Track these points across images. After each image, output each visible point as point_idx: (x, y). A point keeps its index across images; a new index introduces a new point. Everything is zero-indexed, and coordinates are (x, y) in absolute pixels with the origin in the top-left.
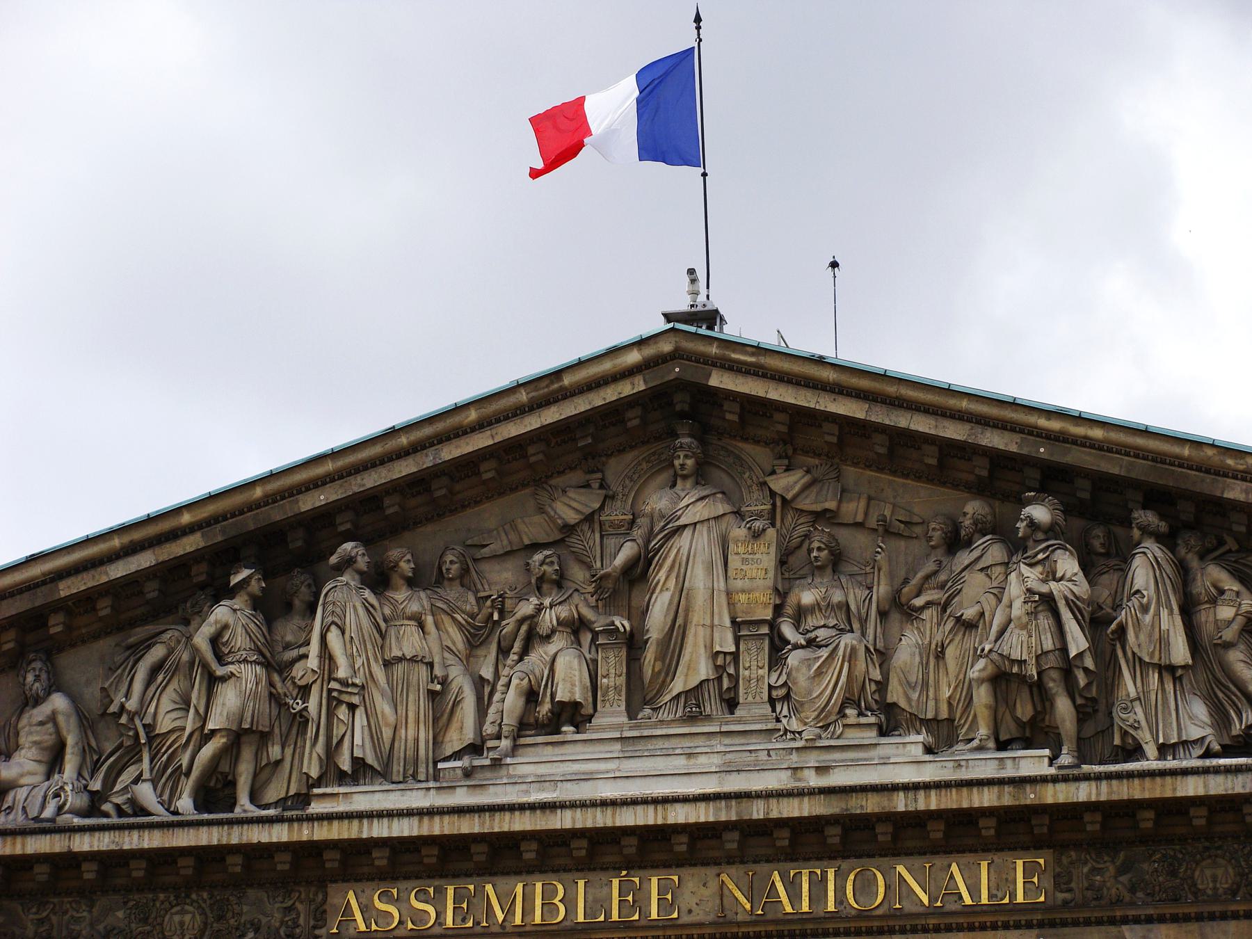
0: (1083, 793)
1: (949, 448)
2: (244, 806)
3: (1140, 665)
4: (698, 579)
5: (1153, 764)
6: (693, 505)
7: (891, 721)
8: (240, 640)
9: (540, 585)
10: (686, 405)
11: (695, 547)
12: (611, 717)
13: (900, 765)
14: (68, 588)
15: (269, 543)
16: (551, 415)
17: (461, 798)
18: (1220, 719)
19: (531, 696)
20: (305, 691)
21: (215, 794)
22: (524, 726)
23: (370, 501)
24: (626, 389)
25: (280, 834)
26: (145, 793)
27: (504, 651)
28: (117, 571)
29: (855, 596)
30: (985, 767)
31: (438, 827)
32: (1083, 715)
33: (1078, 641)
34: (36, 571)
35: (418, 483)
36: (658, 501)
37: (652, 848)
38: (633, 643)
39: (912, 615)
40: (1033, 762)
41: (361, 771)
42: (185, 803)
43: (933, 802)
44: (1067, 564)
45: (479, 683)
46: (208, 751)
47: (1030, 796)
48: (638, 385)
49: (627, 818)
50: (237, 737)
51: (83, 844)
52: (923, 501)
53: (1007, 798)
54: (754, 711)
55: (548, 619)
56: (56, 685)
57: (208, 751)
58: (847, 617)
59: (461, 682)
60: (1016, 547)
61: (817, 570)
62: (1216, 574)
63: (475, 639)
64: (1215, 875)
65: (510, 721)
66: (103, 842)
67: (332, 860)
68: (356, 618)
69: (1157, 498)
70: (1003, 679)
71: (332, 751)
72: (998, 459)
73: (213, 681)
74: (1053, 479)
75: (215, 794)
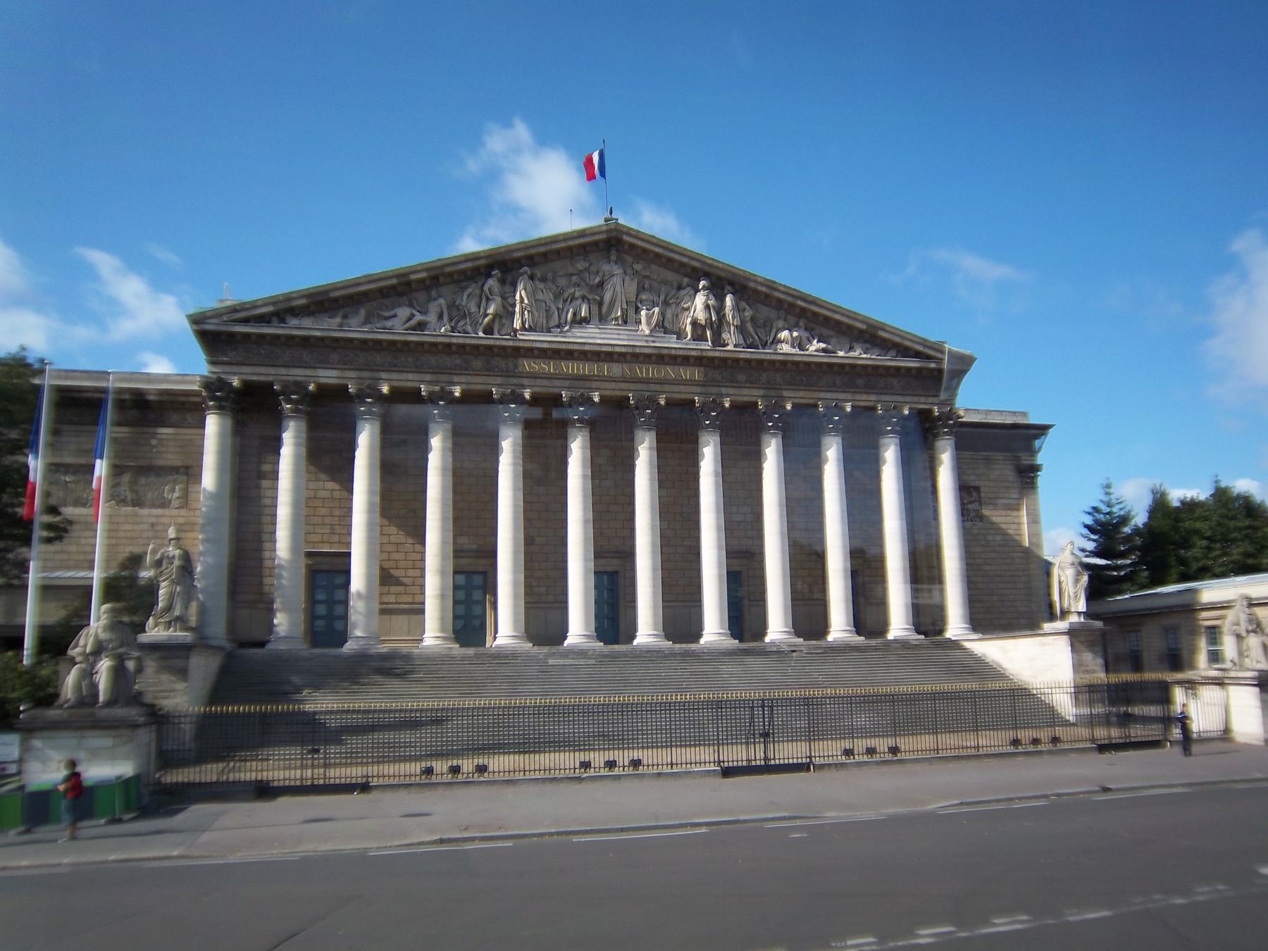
0: (717, 354)
1: (682, 264)
4: (618, 288)
5: (730, 348)
6: (618, 270)
10: (612, 244)
11: (617, 280)
13: (671, 342)
14: (448, 270)
16: (582, 241)
19: (575, 314)
25: (511, 343)
26: (469, 328)
27: (565, 301)
28: (462, 267)
31: (554, 346)
32: (713, 335)
34: (439, 264)
35: (544, 255)
36: (606, 267)
38: (600, 304)
41: (531, 329)
42: (481, 334)
43: (681, 353)
46: (487, 319)
47: (704, 354)
48: (604, 236)
52: (670, 276)
56: (440, 296)
57: (487, 319)
59: (553, 308)
62: (743, 304)
63: (557, 296)
64: (741, 377)
66: (461, 341)
67: (522, 352)
69: (731, 283)
72: (694, 269)
73: (488, 299)
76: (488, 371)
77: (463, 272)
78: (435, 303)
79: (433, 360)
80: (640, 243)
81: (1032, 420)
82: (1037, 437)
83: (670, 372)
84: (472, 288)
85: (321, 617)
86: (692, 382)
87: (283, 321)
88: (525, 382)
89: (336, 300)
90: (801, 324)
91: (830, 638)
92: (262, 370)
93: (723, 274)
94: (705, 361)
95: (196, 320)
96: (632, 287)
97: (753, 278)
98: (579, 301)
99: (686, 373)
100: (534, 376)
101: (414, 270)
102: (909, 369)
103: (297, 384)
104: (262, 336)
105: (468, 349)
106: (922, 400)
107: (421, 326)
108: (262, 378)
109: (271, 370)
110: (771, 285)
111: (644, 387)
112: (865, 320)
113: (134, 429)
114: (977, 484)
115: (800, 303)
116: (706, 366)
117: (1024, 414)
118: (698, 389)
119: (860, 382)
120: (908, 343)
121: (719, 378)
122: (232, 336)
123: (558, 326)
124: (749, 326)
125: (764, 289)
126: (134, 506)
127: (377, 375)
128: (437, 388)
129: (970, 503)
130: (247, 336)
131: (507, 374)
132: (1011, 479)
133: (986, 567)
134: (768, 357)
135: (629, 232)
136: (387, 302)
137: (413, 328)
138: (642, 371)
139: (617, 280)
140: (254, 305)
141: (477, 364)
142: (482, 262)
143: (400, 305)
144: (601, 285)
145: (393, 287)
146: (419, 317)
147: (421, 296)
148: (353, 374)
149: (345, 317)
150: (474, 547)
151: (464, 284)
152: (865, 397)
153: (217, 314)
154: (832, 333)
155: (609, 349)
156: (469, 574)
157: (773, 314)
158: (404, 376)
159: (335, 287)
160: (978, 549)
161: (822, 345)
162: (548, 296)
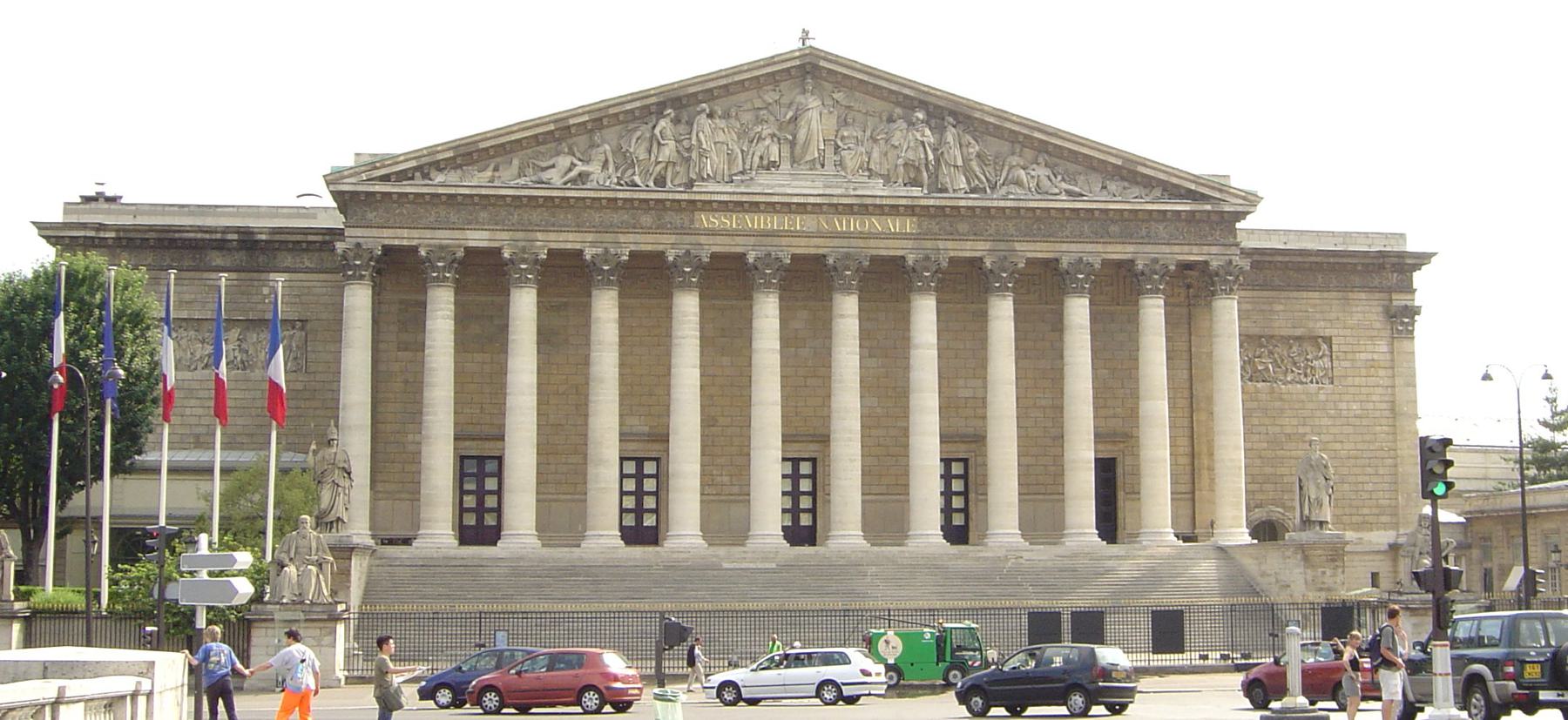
0: (931, 202)
3: (947, 163)
4: (814, 124)
6: (814, 102)
7: (872, 174)
8: (669, 133)
9: (761, 121)
10: (809, 70)
11: (814, 115)
12: (785, 166)
14: (611, 111)
15: (679, 103)
16: (769, 70)
18: (968, 182)
20: (689, 150)
21: (660, 181)
22: (760, 167)
23: (710, 90)
25: (685, 197)
26: (637, 179)
28: (628, 107)
29: (860, 134)
33: (931, 157)
36: (800, 99)
37: (802, 208)
38: (793, 144)
39: (876, 141)
40: (916, 192)
43: (888, 202)
44: (928, 132)
46: (659, 168)
47: (916, 202)
49: (795, 200)
52: (878, 105)
53: (910, 202)
54: (830, 169)
56: (604, 141)
57: (659, 168)
58: (858, 142)
60: (911, 124)
61: (846, 123)
63: (742, 134)
64: (963, 227)
66: (627, 195)
68: (707, 129)
69: (953, 113)
70: (905, 165)
72: (906, 96)
74: (923, 105)
75: (660, 181)
76: (660, 228)
77: (632, 111)
78: (601, 149)
79: (597, 217)
80: (839, 69)
81: (1412, 246)
82: (1417, 267)
83: (876, 223)
84: (644, 130)
85: (469, 510)
86: (903, 236)
87: (426, 176)
88: (703, 240)
89: (486, 149)
90: (1040, 160)
91: (1070, 544)
92: (405, 233)
93: (940, 103)
94: (917, 210)
95: (332, 179)
96: (832, 122)
97: (980, 107)
98: (768, 142)
99: (894, 224)
100: (713, 233)
101: (573, 113)
102: (1179, 212)
103: (442, 247)
104: (400, 195)
105: (636, 204)
106: (1195, 249)
107: (583, 177)
108: (405, 243)
109: (415, 234)
110: (1001, 115)
111: (845, 242)
112: (1118, 154)
113: (243, 275)
114: (1327, 333)
115: (1037, 135)
116: (919, 216)
117: (1402, 236)
118: (910, 244)
119: (1114, 229)
120: (1175, 181)
121: (936, 229)
122: (373, 194)
123: (742, 173)
124: (974, 164)
125: (992, 120)
126: (244, 369)
127: (531, 235)
128: (600, 251)
129: (1317, 358)
130: (390, 194)
131: (682, 231)
132: (1378, 325)
133: (1338, 446)
134: (995, 204)
135: (827, 57)
136: (542, 148)
137: (573, 181)
138: (842, 224)
139: (814, 115)
140: (394, 159)
141: (646, 219)
142: (653, 100)
143: (558, 154)
144: (795, 119)
145: (552, 132)
146: (581, 167)
147: (582, 140)
148: (505, 235)
149: (496, 169)
150: (646, 429)
151: (631, 126)
152: (1119, 248)
153: (354, 172)
154: (1080, 168)
156: (640, 462)
157: (1005, 147)
158: (563, 237)
159: (485, 136)
160: (1325, 421)
161: (1064, 186)
162: (729, 138)
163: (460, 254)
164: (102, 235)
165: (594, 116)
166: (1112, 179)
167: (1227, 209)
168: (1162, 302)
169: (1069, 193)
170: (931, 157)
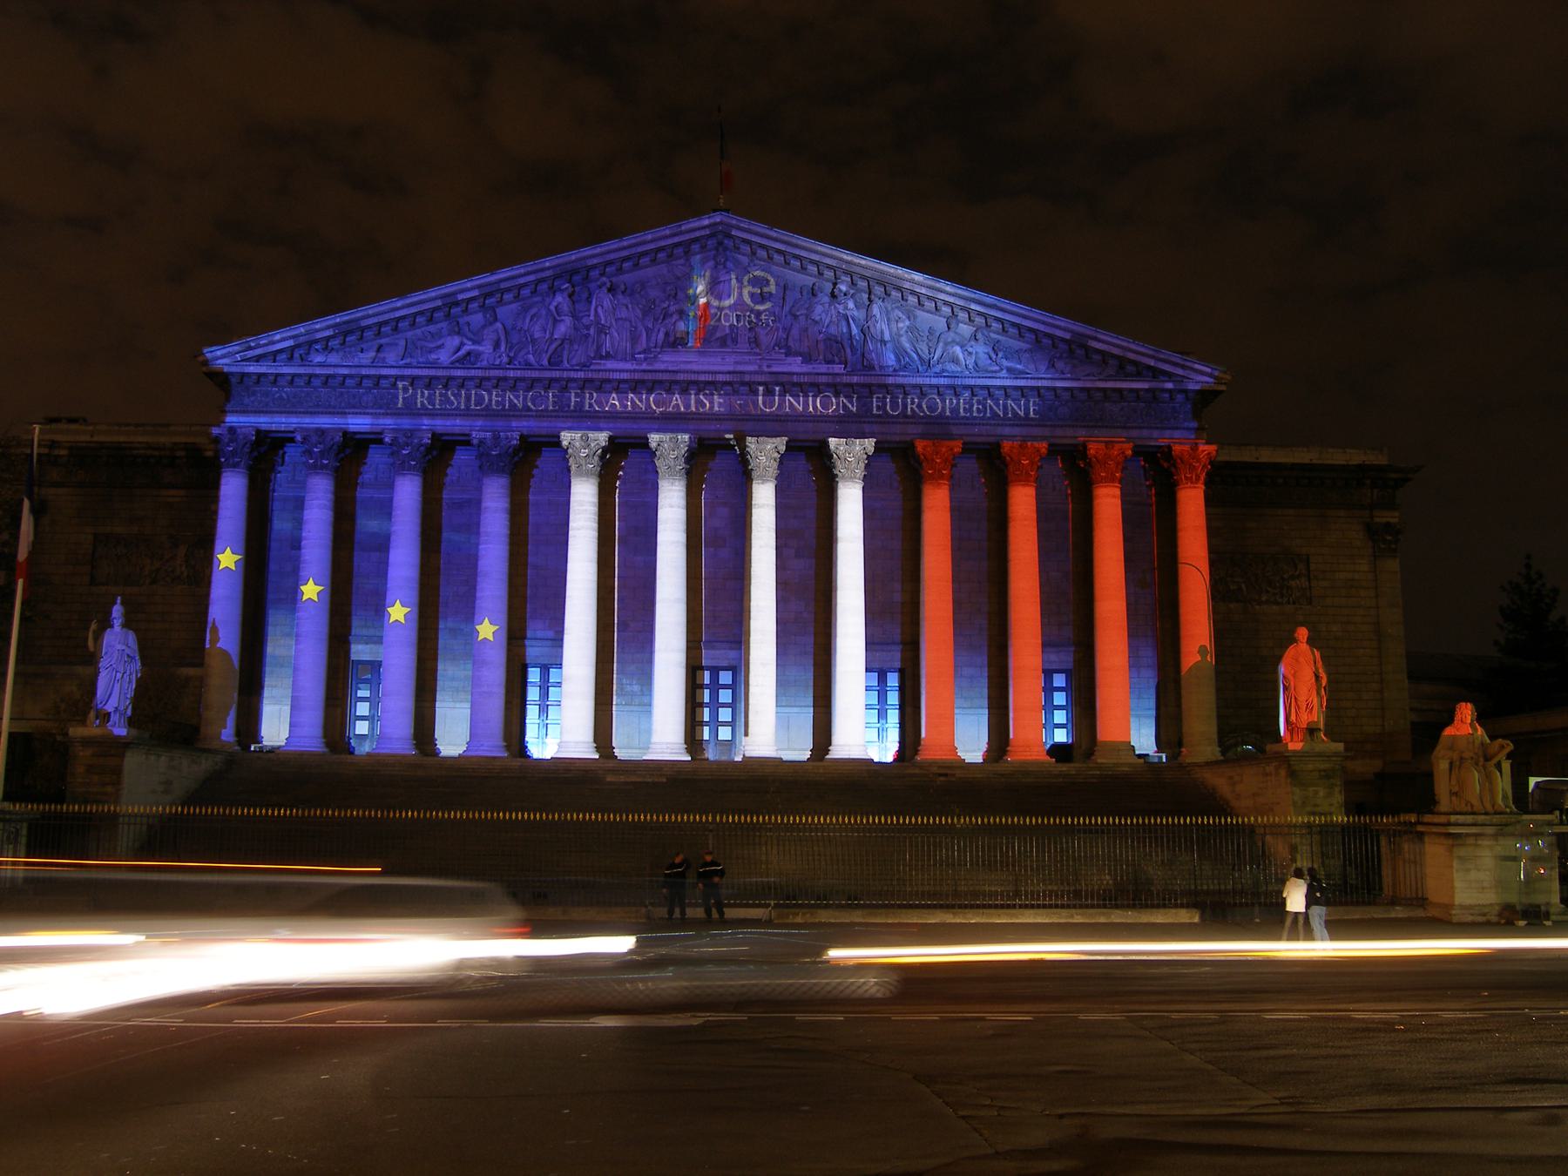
0: (855, 379)
2: (566, 364)
8: (566, 308)
9: (668, 298)
13: (795, 365)
17: (644, 366)
19: (667, 334)
20: (588, 328)
21: (554, 362)
24: (703, 233)
27: (656, 320)
30: (823, 368)
31: (637, 376)
40: (839, 368)
41: (608, 356)
42: (545, 362)
45: (647, 329)
49: (702, 378)
50: (563, 341)
51: (511, 374)
53: (829, 379)
55: (672, 309)
57: (554, 346)
59: (641, 327)
63: (645, 314)
65: (660, 342)
66: (519, 373)
68: (607, 303)
71: (599, 348)
73: (556, 321)
75: (554, 362)
87: (304, 360)
98: (675, 317)
102: (1136, 391)
123: (644, 352)
136: (432, 328)
137: (460, 361)
155: (710, 378)
161: (1005, 363)
163: (338, 438)
164: (56, 452)
165: (487, 290)
166: (1060, 358)
167: (1191, 386)
168: (1118, 492)
169: (1009, 370)
170: (855, 330)
